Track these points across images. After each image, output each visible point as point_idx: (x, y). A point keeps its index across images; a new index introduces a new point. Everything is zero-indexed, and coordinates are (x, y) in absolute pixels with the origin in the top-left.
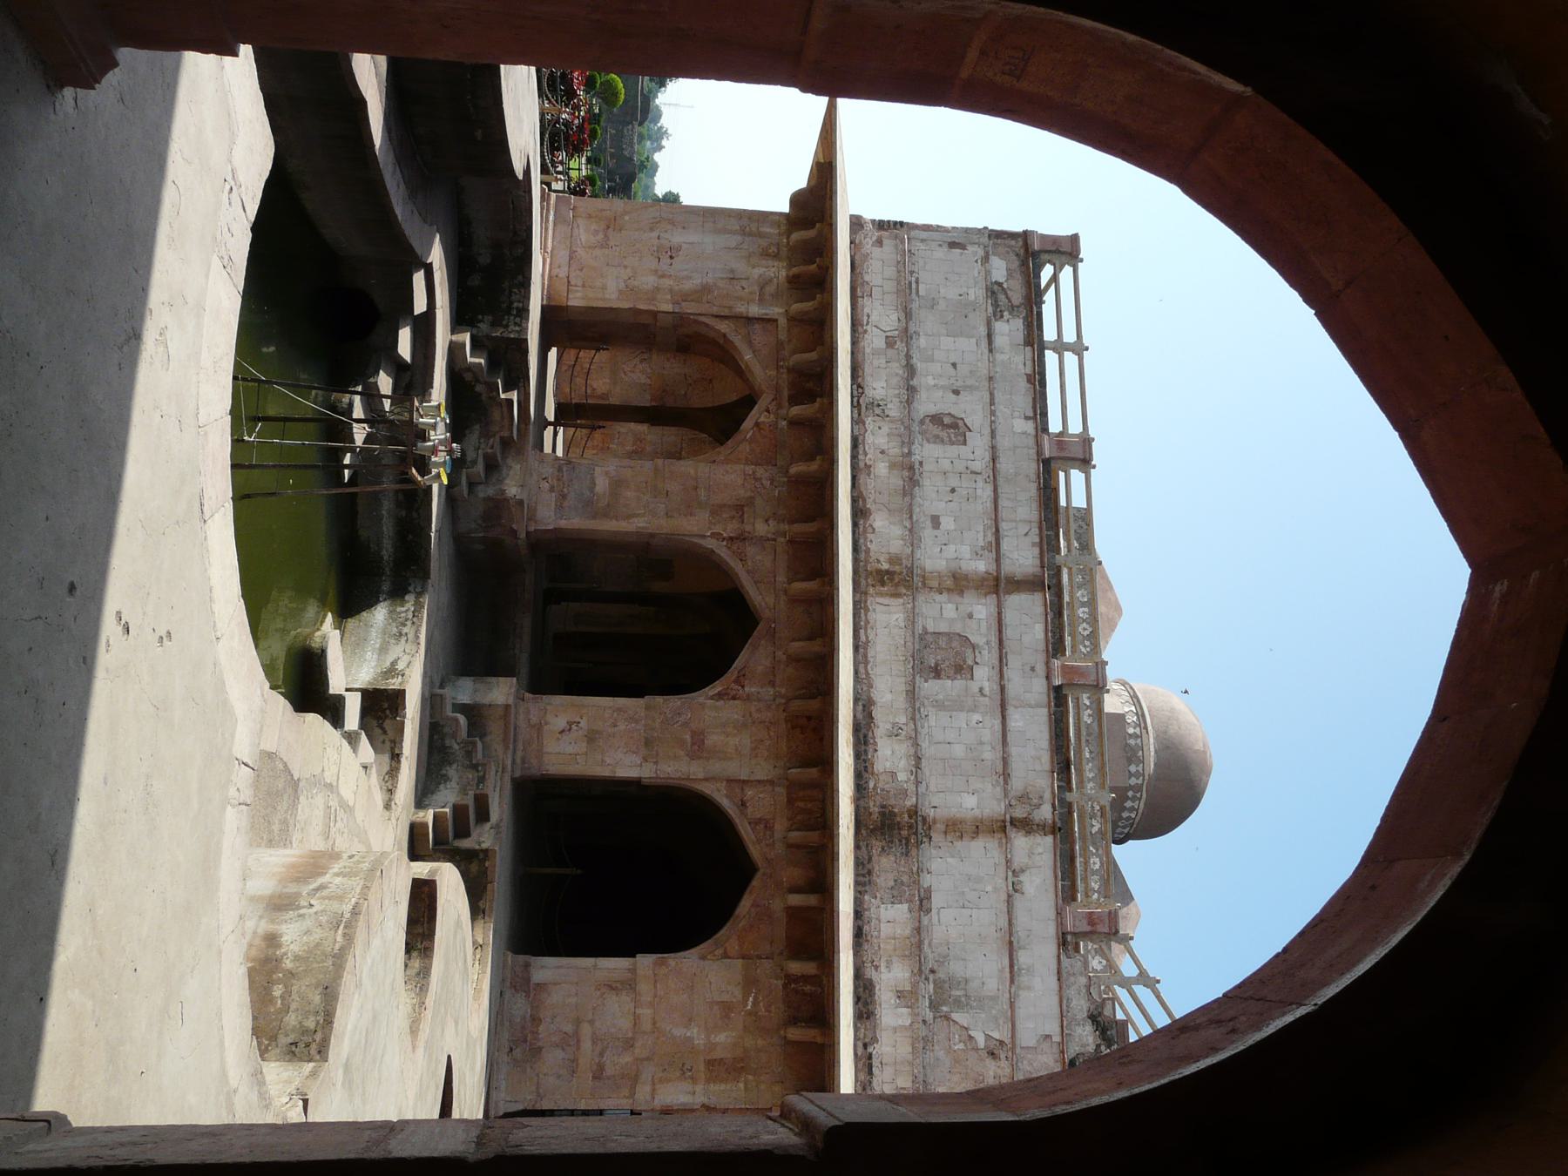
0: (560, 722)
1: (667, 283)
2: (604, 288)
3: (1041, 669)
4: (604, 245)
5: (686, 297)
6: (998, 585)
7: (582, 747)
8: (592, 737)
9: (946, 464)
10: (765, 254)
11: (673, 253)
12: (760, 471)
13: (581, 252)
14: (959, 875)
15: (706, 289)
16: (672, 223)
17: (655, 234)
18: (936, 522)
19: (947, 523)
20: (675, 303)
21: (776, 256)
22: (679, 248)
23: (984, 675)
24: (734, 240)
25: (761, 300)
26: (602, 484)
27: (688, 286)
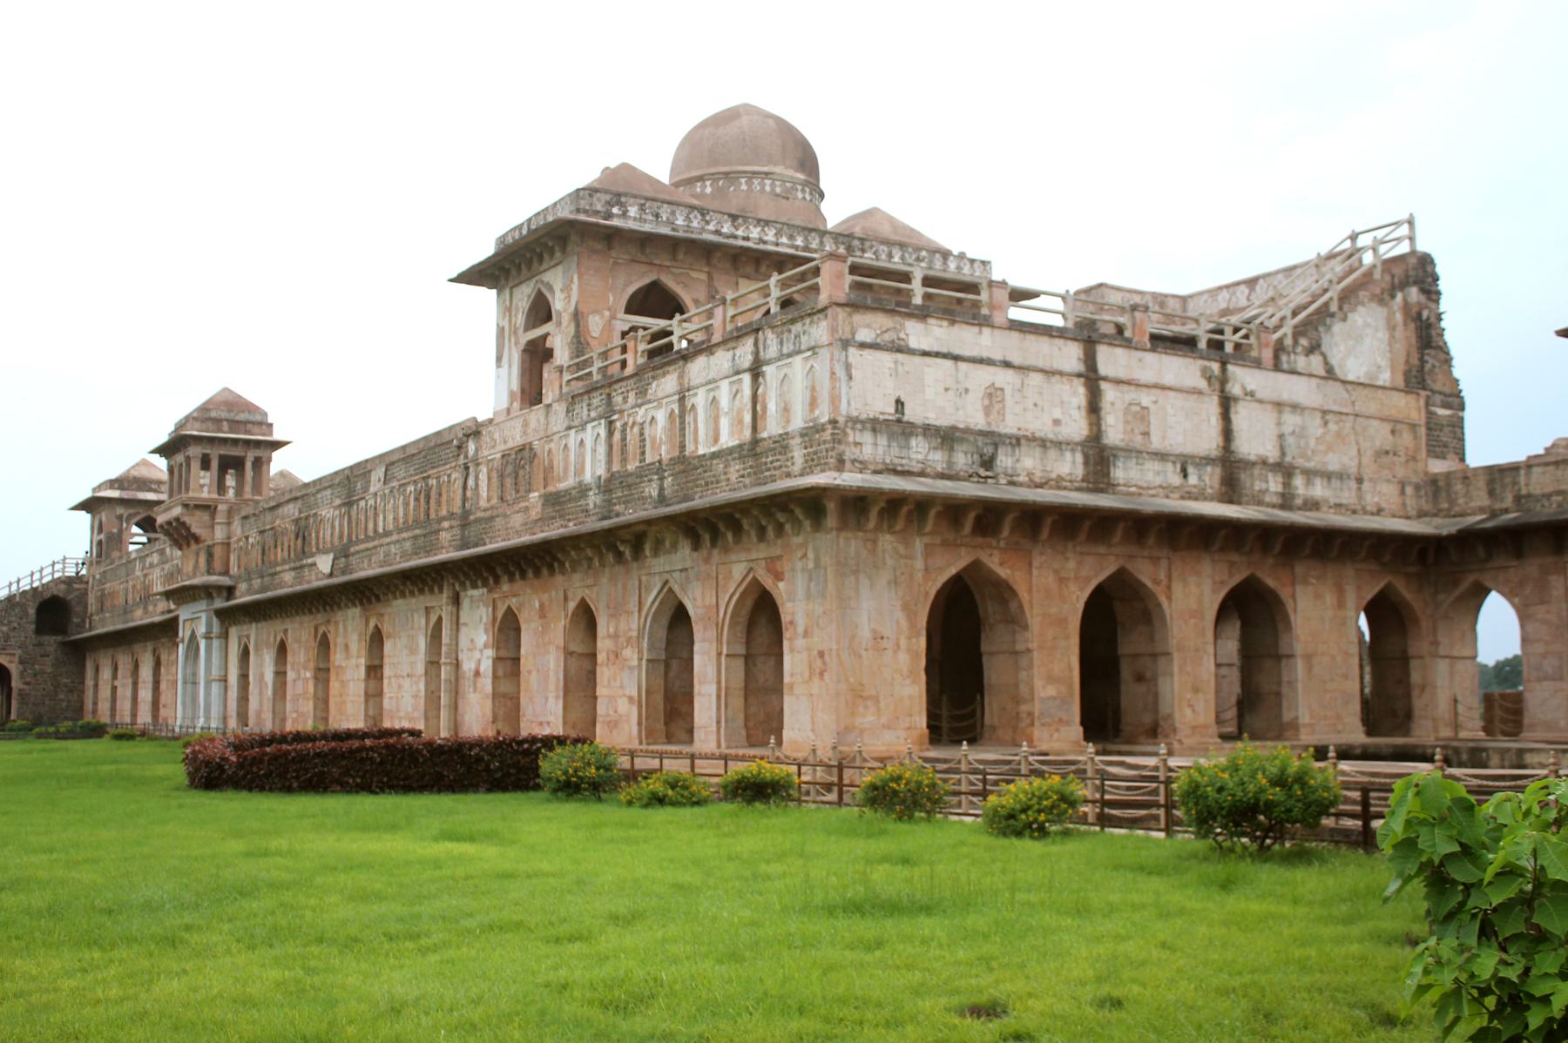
0: (1188, 712)
1: (903, 642)
2: (911, 697)
3: (1140, 354)
4: (876, 700)
5: (912, 626)
6: (1092, 378)
7: (1200, 695)
8: (1196, 690)
9: (1018, 409)
10: (873, 551)
11: (878, 637)
12: (1035, 563)
13: (883, 720)
14: (1256, 437)
15: (905, 607)
16: (853, 637)
17: (864, 653)
18: (1057, 422)
19: (1057, 414)
20: (918, 635)
21: (875, 542)
22: (874, 631)
23: (1146, 399)
24: (864, 582)
25: (911, 557)
26: (1051, 691)
27: (904, 623)
